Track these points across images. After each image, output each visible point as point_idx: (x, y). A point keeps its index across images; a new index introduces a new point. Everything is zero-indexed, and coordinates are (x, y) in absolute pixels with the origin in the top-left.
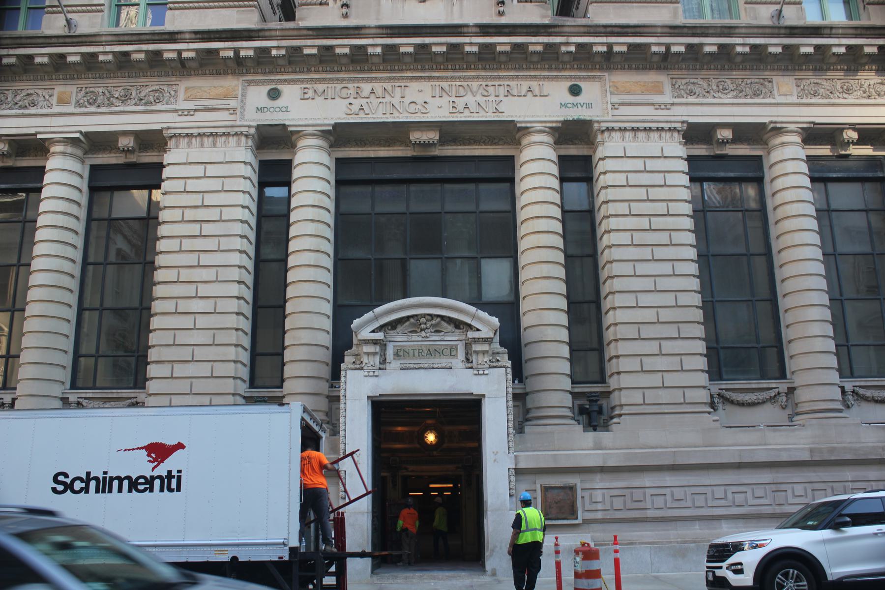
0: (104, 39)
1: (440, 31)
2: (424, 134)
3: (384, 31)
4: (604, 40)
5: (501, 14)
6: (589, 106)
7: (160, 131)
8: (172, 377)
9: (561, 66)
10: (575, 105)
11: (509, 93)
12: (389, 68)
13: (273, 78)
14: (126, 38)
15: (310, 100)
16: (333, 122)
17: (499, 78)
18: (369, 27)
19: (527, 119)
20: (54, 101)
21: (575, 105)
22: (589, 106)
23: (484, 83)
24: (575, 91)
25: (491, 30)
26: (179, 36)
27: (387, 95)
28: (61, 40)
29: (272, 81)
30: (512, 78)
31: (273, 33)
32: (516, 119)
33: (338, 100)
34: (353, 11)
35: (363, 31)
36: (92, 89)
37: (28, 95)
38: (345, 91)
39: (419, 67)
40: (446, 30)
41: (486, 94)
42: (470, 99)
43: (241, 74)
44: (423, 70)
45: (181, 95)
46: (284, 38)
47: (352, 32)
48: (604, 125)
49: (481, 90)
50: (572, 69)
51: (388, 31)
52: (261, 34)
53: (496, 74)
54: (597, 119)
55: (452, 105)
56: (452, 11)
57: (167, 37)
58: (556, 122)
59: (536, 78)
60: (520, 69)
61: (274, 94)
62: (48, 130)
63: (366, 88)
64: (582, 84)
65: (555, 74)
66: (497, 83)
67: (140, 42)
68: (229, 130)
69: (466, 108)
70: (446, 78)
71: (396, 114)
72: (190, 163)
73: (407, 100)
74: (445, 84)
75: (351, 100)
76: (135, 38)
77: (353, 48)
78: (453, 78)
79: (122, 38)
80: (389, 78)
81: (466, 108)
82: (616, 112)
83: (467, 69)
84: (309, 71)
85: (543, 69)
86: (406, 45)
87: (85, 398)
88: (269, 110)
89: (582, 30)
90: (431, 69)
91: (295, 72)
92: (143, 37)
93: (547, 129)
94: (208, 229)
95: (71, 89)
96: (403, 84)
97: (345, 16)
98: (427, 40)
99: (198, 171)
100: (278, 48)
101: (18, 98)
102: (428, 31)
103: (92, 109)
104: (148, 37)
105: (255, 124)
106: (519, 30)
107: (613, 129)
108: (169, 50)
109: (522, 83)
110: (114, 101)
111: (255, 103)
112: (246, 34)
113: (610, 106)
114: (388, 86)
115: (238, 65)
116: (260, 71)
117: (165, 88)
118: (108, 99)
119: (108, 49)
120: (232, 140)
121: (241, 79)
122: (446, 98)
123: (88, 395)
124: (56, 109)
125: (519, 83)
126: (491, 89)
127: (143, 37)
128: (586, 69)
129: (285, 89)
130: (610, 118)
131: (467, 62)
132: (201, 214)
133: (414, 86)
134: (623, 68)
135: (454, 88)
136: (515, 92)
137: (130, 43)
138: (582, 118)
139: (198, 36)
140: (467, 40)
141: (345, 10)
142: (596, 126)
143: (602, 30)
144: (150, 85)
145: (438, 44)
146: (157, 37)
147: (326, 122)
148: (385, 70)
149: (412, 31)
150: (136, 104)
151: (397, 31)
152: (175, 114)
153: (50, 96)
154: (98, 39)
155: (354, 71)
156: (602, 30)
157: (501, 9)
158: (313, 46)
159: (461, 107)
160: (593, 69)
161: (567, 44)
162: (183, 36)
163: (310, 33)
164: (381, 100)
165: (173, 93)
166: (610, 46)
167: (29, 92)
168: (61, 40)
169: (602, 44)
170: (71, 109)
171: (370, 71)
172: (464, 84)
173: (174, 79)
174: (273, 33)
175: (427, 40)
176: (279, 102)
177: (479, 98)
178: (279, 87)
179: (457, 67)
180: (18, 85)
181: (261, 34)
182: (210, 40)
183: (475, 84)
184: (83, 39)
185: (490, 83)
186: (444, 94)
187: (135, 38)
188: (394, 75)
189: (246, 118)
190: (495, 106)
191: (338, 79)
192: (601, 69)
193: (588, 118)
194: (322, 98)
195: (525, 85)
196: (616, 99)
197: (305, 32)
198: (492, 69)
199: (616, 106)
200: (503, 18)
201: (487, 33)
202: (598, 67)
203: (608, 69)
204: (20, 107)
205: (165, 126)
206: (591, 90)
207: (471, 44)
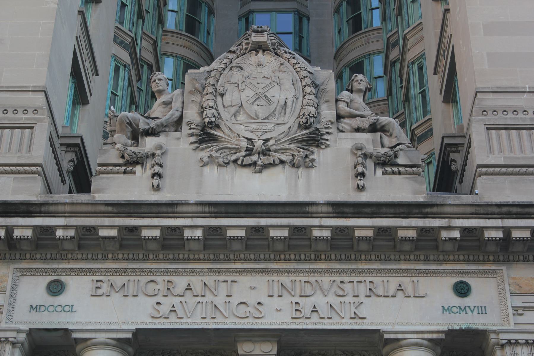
1: (280, 209)
2: (257, 346)
3: (207, 209)
4: (498, 223)
5: (360, 189)
6: (482, 310)
9: (441, 257)
10: (463, 309)
11: (371, 293)
12: (212, 257)
15: (104, 298)
16: (133, 328)
17: (358, 272)
18: (187, 204)
19: (397, 328)
21: (463, 309)
22: (482, 310)
23: (338, 279)
24: (462, 290)
25: (347, 210)
27: (208, 293)
30: (376, 272)
31: (60, 208)
32: (382, 327)
33: (142, 298)
34: (166, 183)
35: (179, 209)
38: (152, 286)
39: (252, 257)
40: (288, 209)
41: (341, 293)
42: (319, 300)
43: (13, 260)
44: (257, 260)
46: (74, 214)
47: (164, 209)
48: (504, 337)
49: (335, 289)
50: (457, 261)
51: (212, 209)
52: (43, 209)
53: (354, 267)
54: (494, 328)
55: (295, 307)
56: (296, 185)
58: (438, 332)
59: (407, 272)
60: (387, 260)
61: (56, 288)
63: (181, 282)
64: (471, 281)
65: (434, 267)
66: (355, 279)
69: (315, 311)
70: (287, 272)
71: (219, 319)
73: (235, 300)
74: (286, 280)
75: (160, 299)
77: (165, 229)
78: (296, 271)
80: (212, 271)
81: (315, 311)
82: (520, 319)
83: (315, 260)
84: (105, 259)
85: (417, 261)
86: (236, 227)
88: (47, 309)
89: (469, 210)
90: (268, 259)
91: (85, 259)
93: (425, 342)
96: (229, 279)
97: (157, 188)
98: (263, 222)
100: (65, 227)
102: (265, 210)
105: (25, 327)
106: (384, 210)
107: (517, 343)
109: (390, 279)
112: (23, 208)
113: (511, 311)
114: (210, 280)
116: (38, 256)
121: (12, 266)
122: (287, 299)
125: (385, 279)
126: (348, 287)
128: (476, 261)
130: (512, 327)
131: (316, 251)
133: (245, 281)
134: (526, 260)
135: (298, 284)
136: (380, 292)
138: (474, 327)
140: (315, 222)
141: (156, 181)
142: (493, 338)
143: (496, 210)
145: (278, 227)
147: (125, 327)
148: (206, 260)
149: (243, 209)
151: (223, 209)
155: (166, 260)
156: (496, 210)
157: (361, 183)
158: (112, 227)
159: (307, 311)
160: (486, 261)
161: (449, 228)
163: (110, 209)
164: (199, 299)
166: (507, 231)
169: (497, 228)
171: (187, 260)
172: (312, 279)
175: (263, 222)
176: (62, 299)
177: (332, 299)
178: (63, 279)
179: (303, 257)
181: (43, 209)
183: (326, 280)
185: (346, 279)
186: (285, 293)
188: (218, 266)
189: (15, 319)
190: (353, 309)
191: (143, 270)
192: (496, 261)
193: (481, 328)
194: (121, 294)
195: (394, 282)
196: (519, 301)
197: (103, 208)
198: (349, 260)
199: (520, 311)
200: (363, 194)
201: (343, 213)
202: (491, 258)
203: (507, 261)
206: (484, 289)
207: (321, 227)
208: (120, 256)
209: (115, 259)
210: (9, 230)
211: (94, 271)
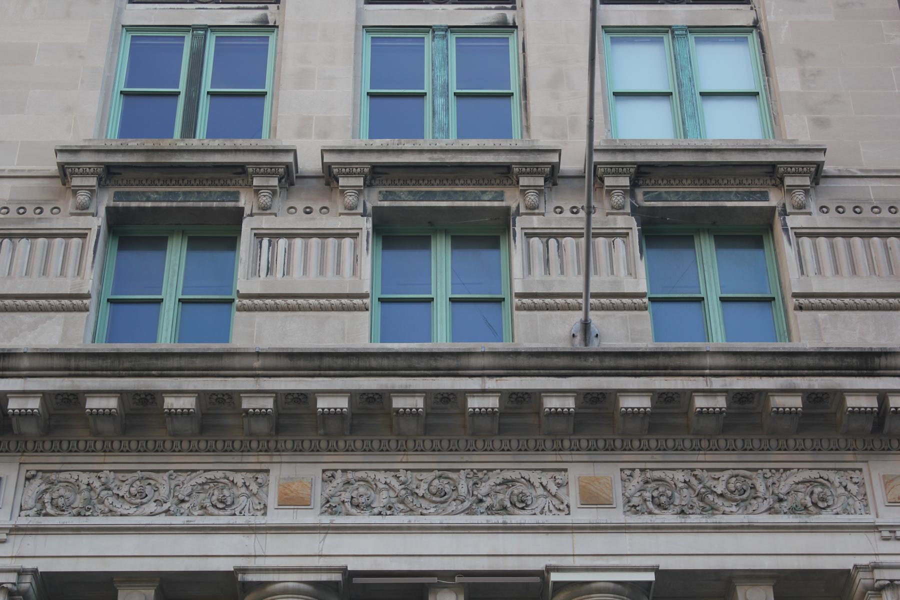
0: (708, 361)
14: (760, 361)
20: (573, 497)
26: (883, 362)
28: (609, 362)
36: (657, 474)
37: (506, 482)
45: (878, 493)
57: (854, 362)
67: (792, 371)
76: (780, 362)
79: (750, 362)
95: (608, 473)
101: (483, 489)
103: (668, 518)
104: (811, 361)
110: (719, 501)
116: (202, 445)
118: (701, 497)
119: (717, 383)
137: (768, 372)
144: (796, 470)
146: (831, 363)
150: (770, 510)
152: (874, 537)
153: (559, 486)
154: (695, 361)
165: (854, 488)
167: (508, 475)
168: (609, 362)
170: (617, 516)
173: (850, 457)
180: (479, 461)
184: (662, 361)
187: (780, 362)
204: (490, 510)
205: (864, 561)
208: (428, 444)
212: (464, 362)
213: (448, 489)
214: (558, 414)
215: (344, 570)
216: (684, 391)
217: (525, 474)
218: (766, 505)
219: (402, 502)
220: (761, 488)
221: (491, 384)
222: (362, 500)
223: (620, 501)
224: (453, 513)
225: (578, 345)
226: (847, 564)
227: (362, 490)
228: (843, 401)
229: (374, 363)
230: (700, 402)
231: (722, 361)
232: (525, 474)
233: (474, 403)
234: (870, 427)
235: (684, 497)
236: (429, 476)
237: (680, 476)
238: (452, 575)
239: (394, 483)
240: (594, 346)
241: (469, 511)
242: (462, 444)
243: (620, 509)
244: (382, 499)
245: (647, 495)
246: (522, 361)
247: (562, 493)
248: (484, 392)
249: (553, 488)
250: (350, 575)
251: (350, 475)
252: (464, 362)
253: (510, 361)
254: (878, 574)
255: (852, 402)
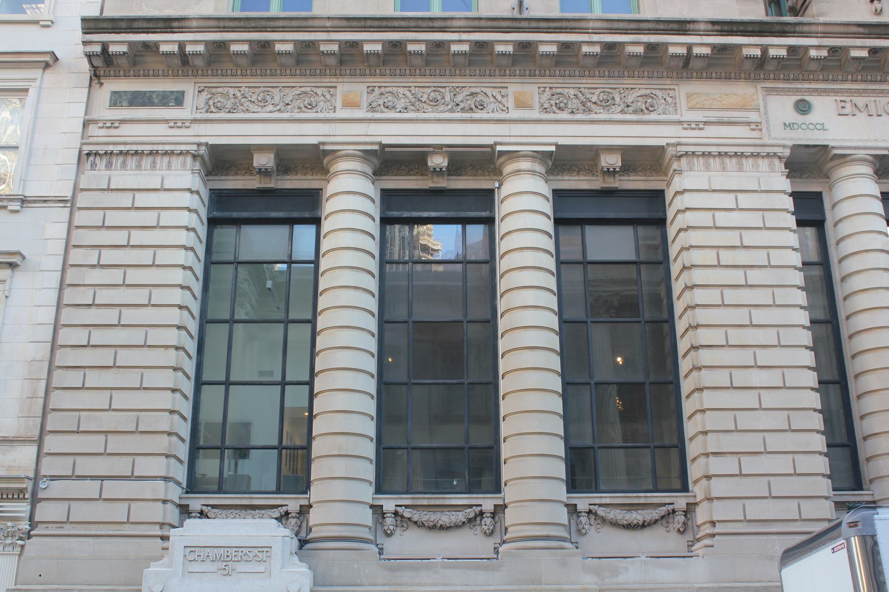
0: (591, 24)
7: (662, 149)
8: (741, 475)
13: (800, 86)
14: (621, 25)
15: (850, 117)
20: (510, 103)
26: (692, 26)
28: (534, 24)
29: (798, 90)
31: (814, 29)
36: (559, 90)
37: (472, 94)
43: (757, 79)
45: (683, 103)
46: (826, 35)
52: (798, 29)
57: (675, 26)
61: (803, 107)
62: (513, 140)
67: (639, 31)
68: (758, 149)
72: (714, 191)
76: (632, 26)
79: (615, 25)
87: (600, 505)
88: (800, 127)
91: (826, 80)
92: (643, 25)
94: (755, 277)
95: (530, 89)
99: (728, 201)
100: (818, 47)
101: (459, 98)
103: (564, 115)
104: (650, 26)
105: (790, 143)
108: (676, 44)
110: (593, 106)
111: (778, 117)
115: (761, 68)
117: (660, 94)
119: (596, 38)
120: (763, 164)
121: (760, 85)
123: (604, 501)
124: (515, 114)
127: (643, 25)
129: (816, 101)
132: (742, 258)
137: (625, 32)
139: (716, 27)
144: (637, 89)
146: (662, 27)
147: (880, 144)
150: (622, 112)
152: (679, 127)
153: (503, 96)
154: (583, 24)
162: (696, 26)
163: (861, 30)
165: (669, 100)
167: (474, 90)
168: (534, 24)
170: (535, 114)
173: (668, 82)
174: (814, 29)
176: (811, 118)
178: (807, 98)
180: (457, 82)
181: (798, 29)
182: (731, 33)
184: (564, 24)
187: (632, 26)
209: (854, 81)
210: (765, 49)
211: (835, 92)
212: (449, 23)
213: (439, 98)
214: (503, 55)
215: (380, 144)
216: (576, 42)
217: (484, 90)
218: (620, 109)
219: (413, 105)
220: (617, 99)
221: (465, 36)
222: (390, 104)
223: (537, 105)
224: (442, 112)
225: (516, 14)
226: (662, 142)
227: (390, 98)
228: (667, 49)
229: (396, 24)
230: (585, 49)
231: (599, 25)
232: (484, 90)
233: (454, 48)
234: (681, 65)
235: (574, 104)
236: (428, 90)
237: (572, 92)
238: (441, 146)
239: (408, 94)
240: (525, 15)
241: (451, 111)
242: (448, 72)
243: (537, 110)
244: (401, 104)
245: (553, 102)
246: (483, 23)
247: (504, 101)
248: (460, 41)
249: (499, 98)
250: (383, 146)
251: (383, 90)
252: (449, 23)
253: (476, 23)
254: (679, 148)
255: (672, 50)
